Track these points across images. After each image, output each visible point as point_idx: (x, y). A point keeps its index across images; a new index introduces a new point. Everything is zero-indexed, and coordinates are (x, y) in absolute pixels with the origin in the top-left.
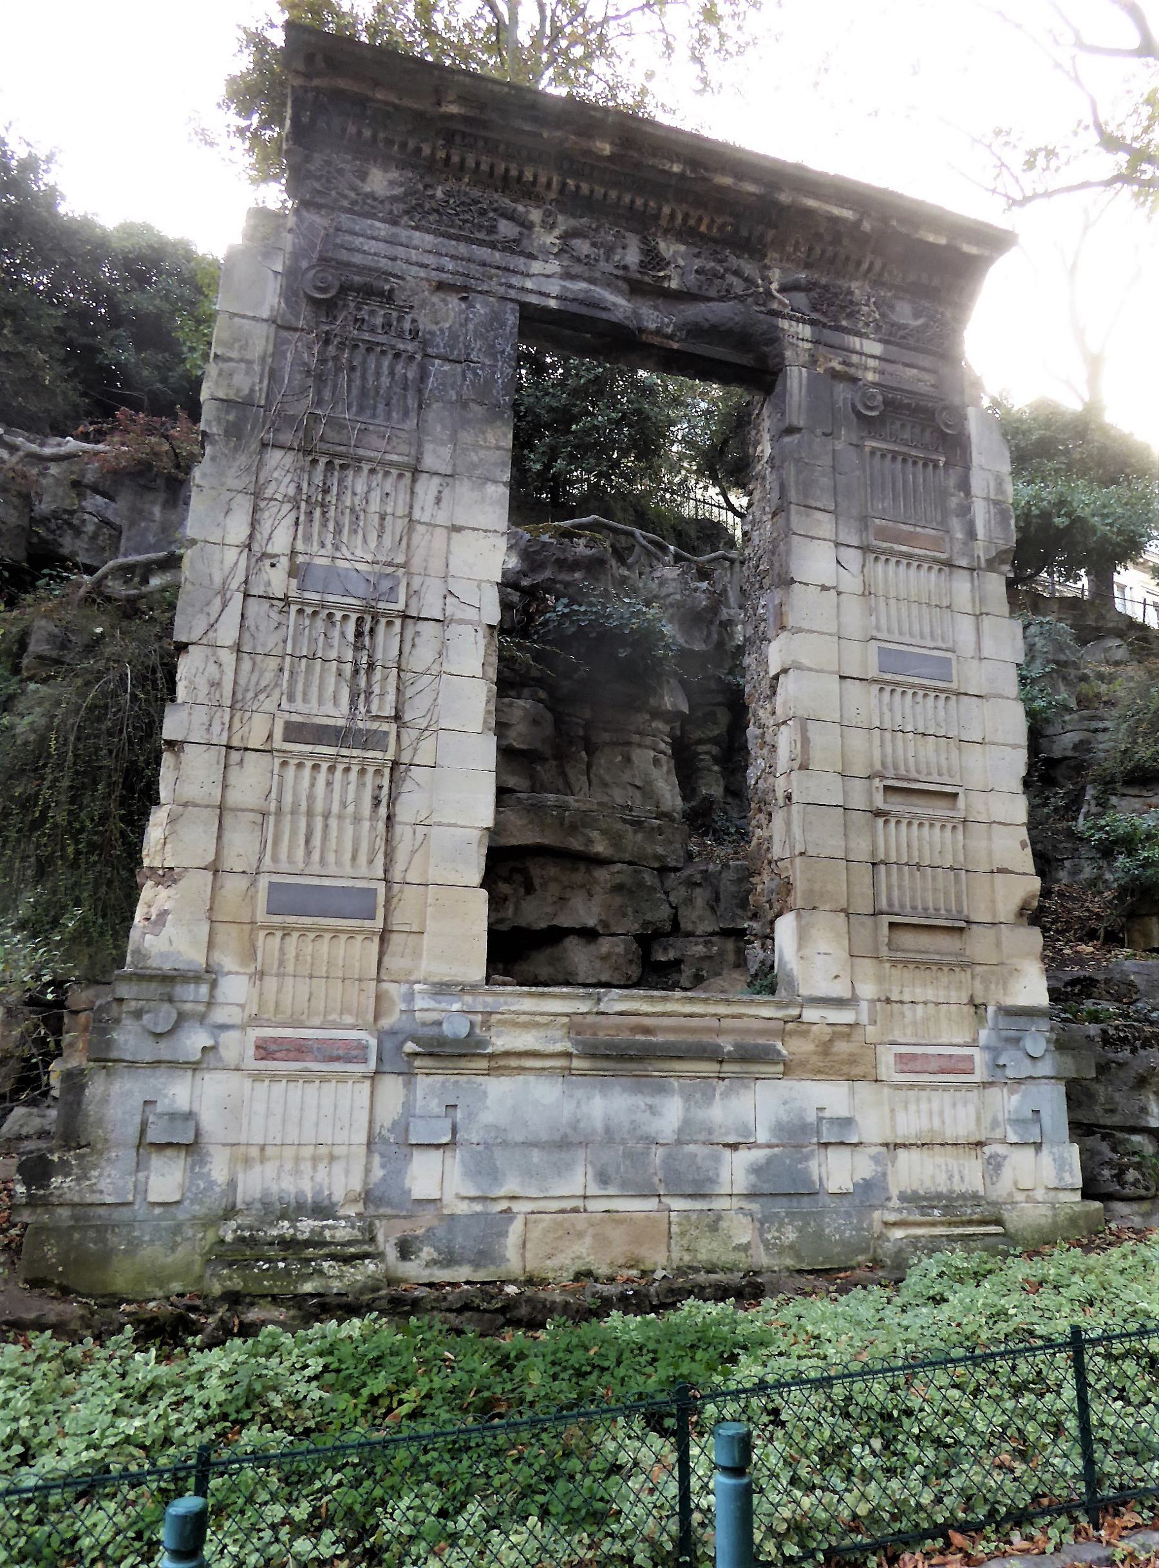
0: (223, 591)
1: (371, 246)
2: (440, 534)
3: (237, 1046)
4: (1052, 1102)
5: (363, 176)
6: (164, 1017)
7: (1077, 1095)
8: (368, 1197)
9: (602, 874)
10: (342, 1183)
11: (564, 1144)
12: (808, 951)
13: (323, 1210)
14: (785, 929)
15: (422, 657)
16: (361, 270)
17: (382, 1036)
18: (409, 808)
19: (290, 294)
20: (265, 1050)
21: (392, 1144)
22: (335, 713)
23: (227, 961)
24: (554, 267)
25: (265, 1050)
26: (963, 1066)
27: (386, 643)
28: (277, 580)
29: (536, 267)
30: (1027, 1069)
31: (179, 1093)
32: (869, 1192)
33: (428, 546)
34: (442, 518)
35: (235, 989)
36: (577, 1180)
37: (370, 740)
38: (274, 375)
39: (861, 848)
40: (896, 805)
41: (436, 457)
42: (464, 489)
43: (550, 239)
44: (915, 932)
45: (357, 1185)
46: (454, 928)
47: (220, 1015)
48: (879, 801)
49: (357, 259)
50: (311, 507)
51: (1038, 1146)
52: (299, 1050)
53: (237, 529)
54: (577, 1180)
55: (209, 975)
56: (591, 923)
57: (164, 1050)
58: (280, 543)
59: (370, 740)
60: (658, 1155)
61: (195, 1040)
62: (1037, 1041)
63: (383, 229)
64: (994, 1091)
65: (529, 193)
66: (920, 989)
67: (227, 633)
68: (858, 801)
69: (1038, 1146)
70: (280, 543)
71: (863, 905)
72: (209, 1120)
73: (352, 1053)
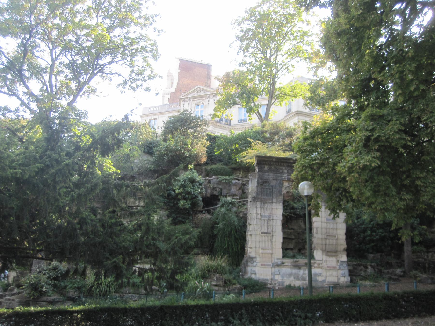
0: (254, 218)
1: (266, 176)
2: (275, 210)
3: (259, 264)
4: (347, 272)
5: (264, 167)
6: (252, 262)
7: (350, 271)
8: (271, 279)
9: (294, 241)
10: (269, 277)
11: (290, 275)
12: (318, 255)
13: (267, 280)
14: (315, 252)
15: (274, 224)
16: (265, 180)
17: (272, 264)
18: (274, 240)
19: (258, 183)
20: (261, 265)
21: (274, 274)
22: (266, 231)
23: (257, 256)
24: (286, 175)
25: (261, 265)
26: (335, 267)
27: (271, 223)
28: (259, 216)
29: (284, 175)
30: (343, 268)
31: (254, 269)
32: (324, 281)
33: (274, 211)
34: (275, 208)
35: (258, 259)
36: (292, 278)
37: (270, 233)
38: (257, 193)
39: (324, 243)
40: (328, 238)
41: (274, 200)
42: (278, 204)
43: (286, 171)
44: (331, 252)
45: (270, 278)
46: (279, 252)
47: (257, 261)
48: (326, 237)
49: (265, 178)
50: (262, 208)
51: (344, 277)
52: (264, 265)
53: (255, 211)
54: (292, 278)
55: (255, 258)
56: (292, 247)
57: (252, 265)
58: (259, 212)
59: (270, 233)
60: (300, 276)
61: (255, 264)
62: (345, 265)
63: (267, 174)
64: (339, 271)
65: (284, 166)
66: (330, 259)
67: (255, 223)
68: (323, 237)
69: (344, 277)
70: (259, 212)
71: (324, 249)
72: (257, 271)
73: (269, 265)
